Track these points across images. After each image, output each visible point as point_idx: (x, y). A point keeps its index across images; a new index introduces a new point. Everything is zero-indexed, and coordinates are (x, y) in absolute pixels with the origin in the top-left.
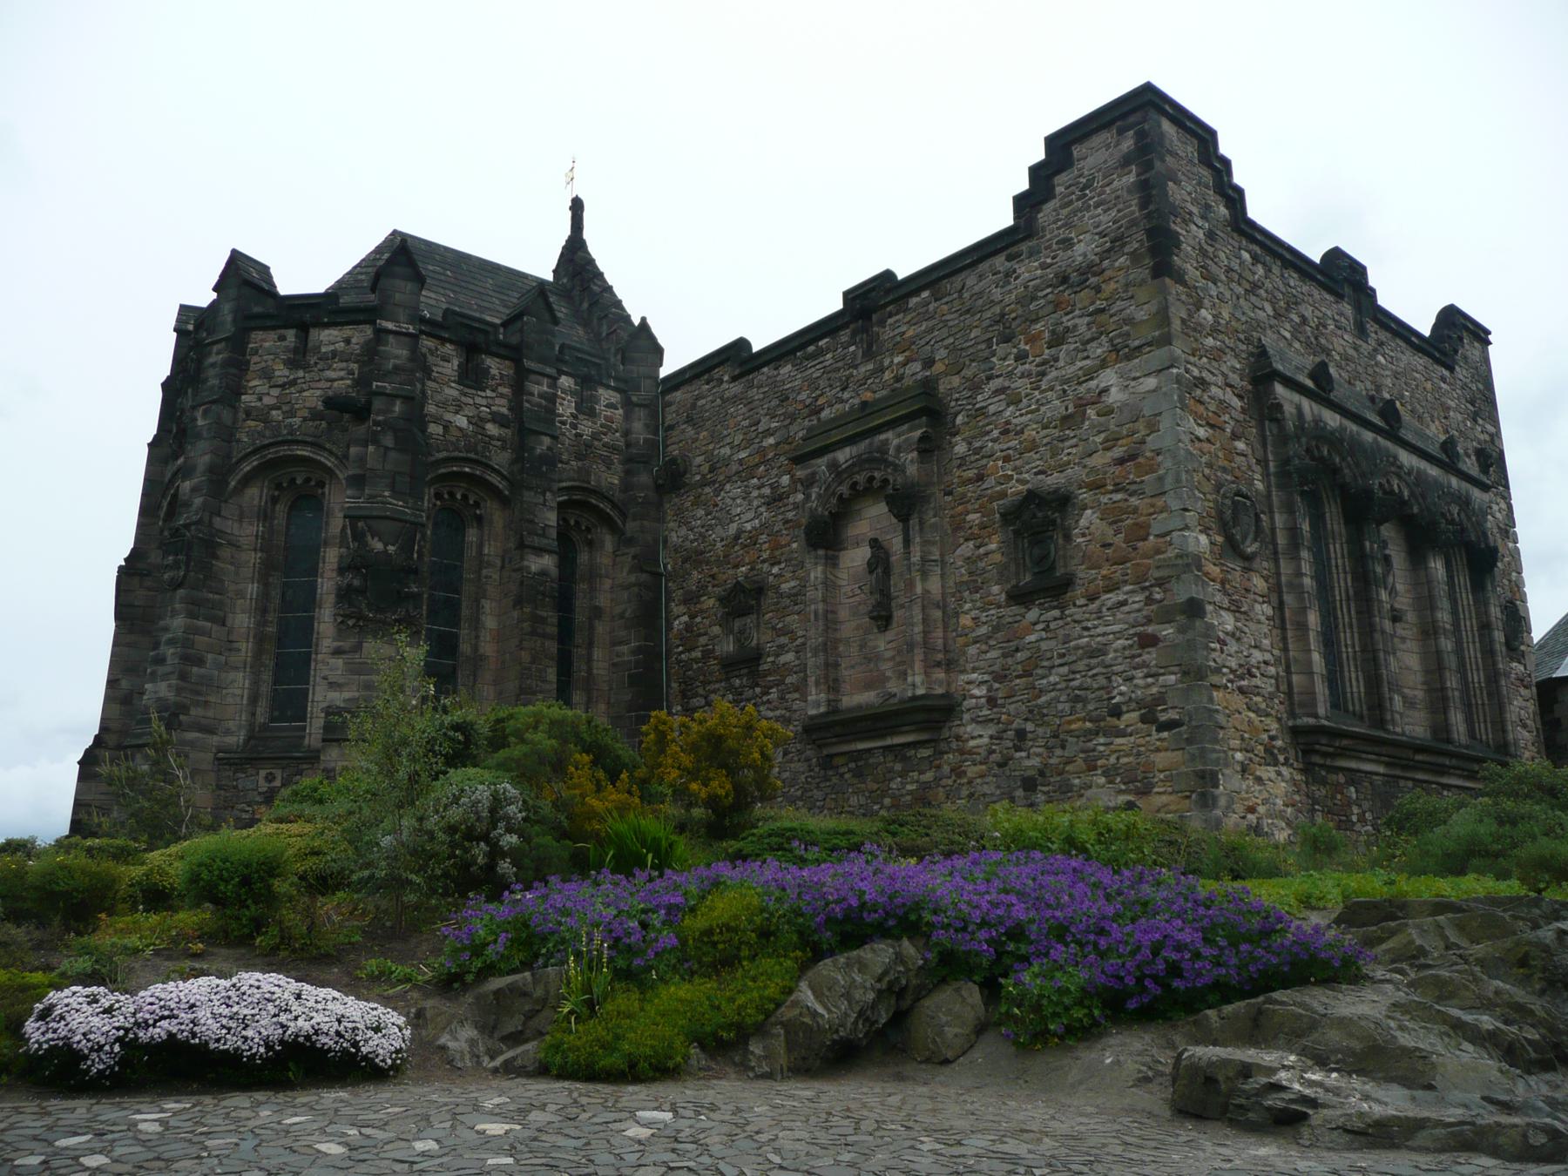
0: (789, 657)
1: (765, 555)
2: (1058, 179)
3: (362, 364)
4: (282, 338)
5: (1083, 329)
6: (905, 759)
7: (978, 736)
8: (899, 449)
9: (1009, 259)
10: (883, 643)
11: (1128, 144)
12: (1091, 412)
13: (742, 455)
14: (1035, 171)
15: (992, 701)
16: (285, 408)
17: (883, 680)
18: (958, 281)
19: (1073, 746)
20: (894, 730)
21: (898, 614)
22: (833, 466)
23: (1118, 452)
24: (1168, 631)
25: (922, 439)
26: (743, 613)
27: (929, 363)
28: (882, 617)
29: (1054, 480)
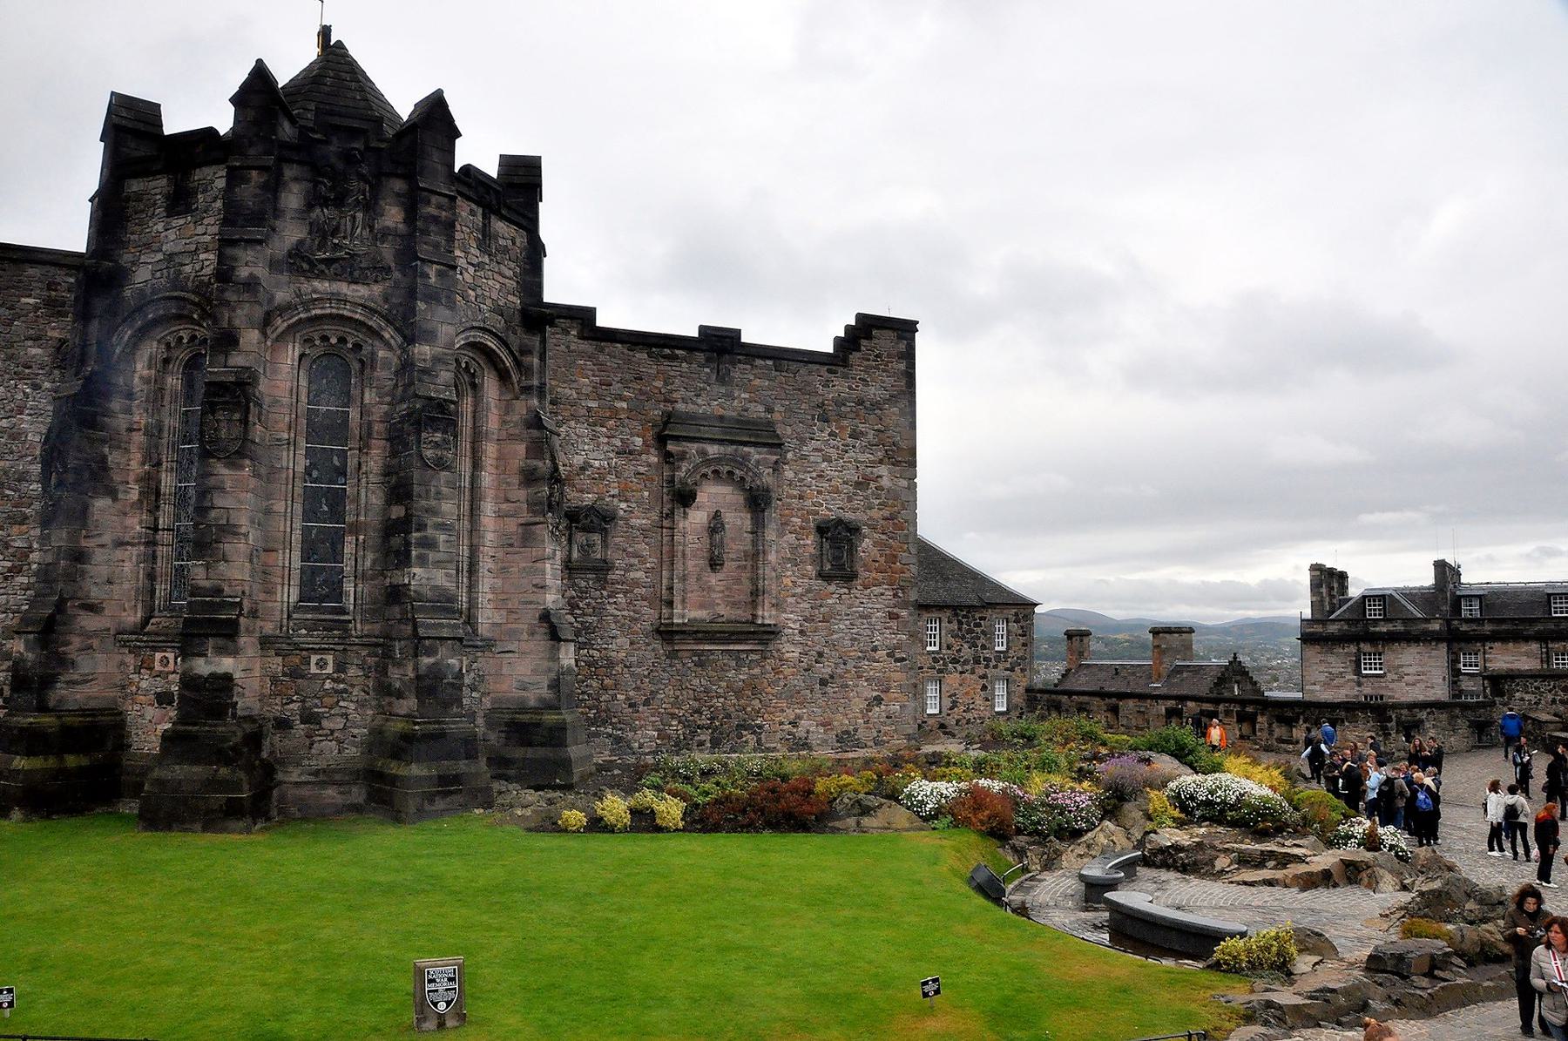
0: (640, 574)
1: (616, 491)
2: (864, 342)
3: (524, 272)
4: (472, 212)
5: (870, 436)
6: (738, 659)
7: (791, 652)
8: (758, 462)
9: (829, 371)
10: (713, 579)
11: (902, 346)
12: (872, 485)
13: (593, 404)
14: (848, 328)
15: (802, 632)
16: (479, 291)
17: (713, 604)
18: (794, 366)
19: (851, 664)
20: (739, 642)
21: (729, 565)
22: (703, 453)
23: (886, 513)
24: (904, 613)
25: (776, 462)
26: (587, 530)
27: (770, 410)
28: (715, 564)
29: (849, 516)
